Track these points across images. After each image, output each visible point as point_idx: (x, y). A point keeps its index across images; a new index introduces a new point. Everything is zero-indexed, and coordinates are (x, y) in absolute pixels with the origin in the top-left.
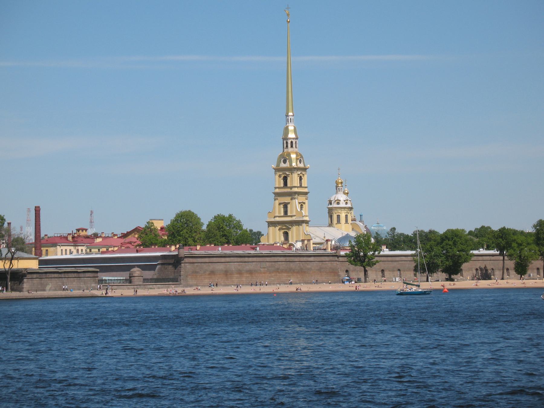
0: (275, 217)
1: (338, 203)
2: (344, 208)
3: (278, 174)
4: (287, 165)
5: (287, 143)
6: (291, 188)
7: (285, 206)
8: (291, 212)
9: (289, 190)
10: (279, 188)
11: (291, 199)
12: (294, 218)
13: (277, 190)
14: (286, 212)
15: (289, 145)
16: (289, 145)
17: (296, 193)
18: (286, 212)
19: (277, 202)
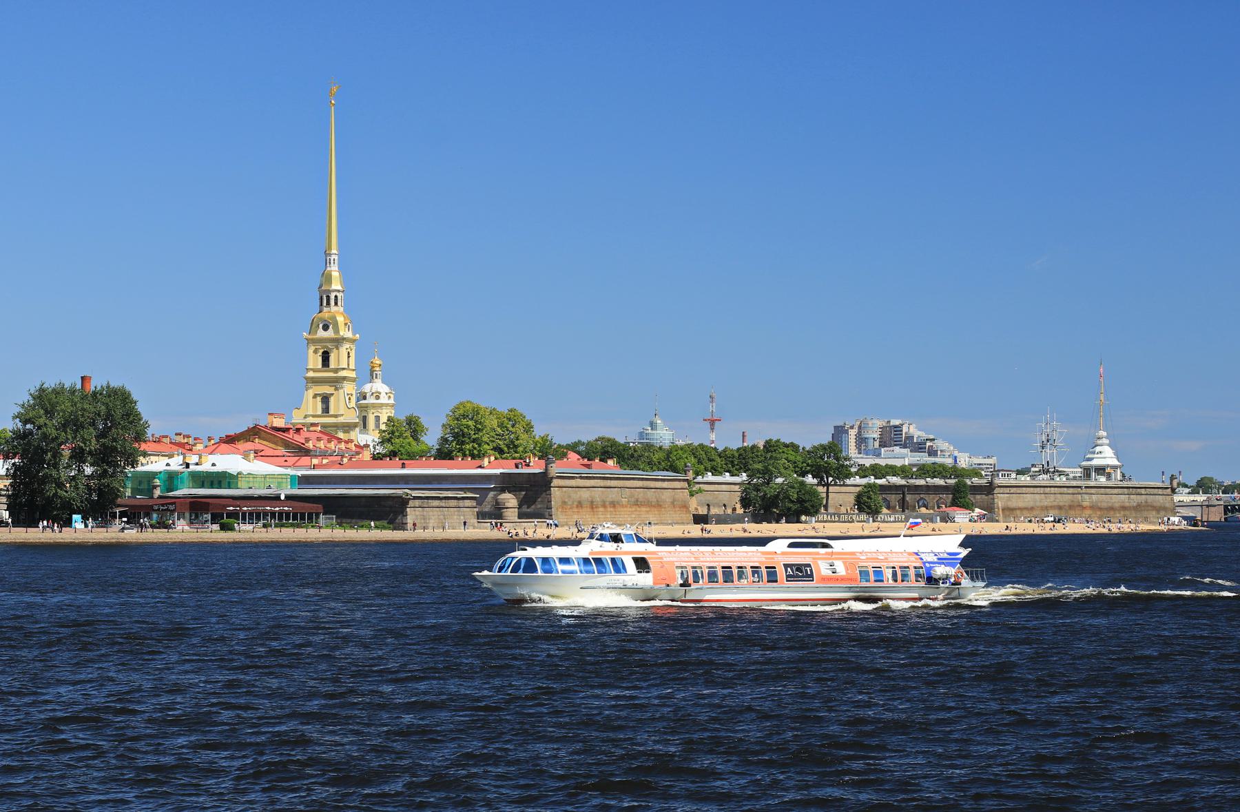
0: (306, 417)
1: (378, 398)
2: (387, 405)
3: (312, 348)
4: (330, 334)
5: (328, 298)
6: (336, 371)
7: (326, 399)
8: (337, 408)
9: (331, 374)
10: (314, 370)
11: (337, 389)
12: (341, 420)
13: (311, 374)
14: (326, 410)
15: (332, 302)
16: (332, 302)
17: (344, 378)
18: (326, 410)
19: (311, 393)
